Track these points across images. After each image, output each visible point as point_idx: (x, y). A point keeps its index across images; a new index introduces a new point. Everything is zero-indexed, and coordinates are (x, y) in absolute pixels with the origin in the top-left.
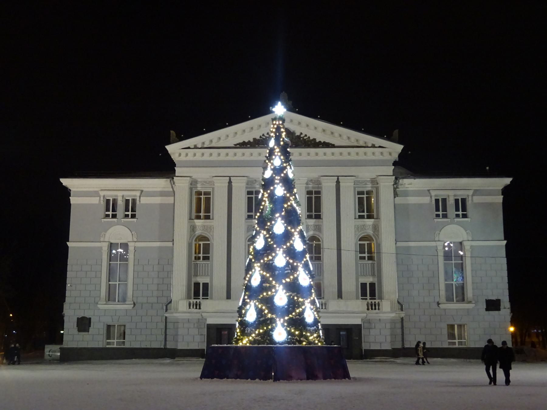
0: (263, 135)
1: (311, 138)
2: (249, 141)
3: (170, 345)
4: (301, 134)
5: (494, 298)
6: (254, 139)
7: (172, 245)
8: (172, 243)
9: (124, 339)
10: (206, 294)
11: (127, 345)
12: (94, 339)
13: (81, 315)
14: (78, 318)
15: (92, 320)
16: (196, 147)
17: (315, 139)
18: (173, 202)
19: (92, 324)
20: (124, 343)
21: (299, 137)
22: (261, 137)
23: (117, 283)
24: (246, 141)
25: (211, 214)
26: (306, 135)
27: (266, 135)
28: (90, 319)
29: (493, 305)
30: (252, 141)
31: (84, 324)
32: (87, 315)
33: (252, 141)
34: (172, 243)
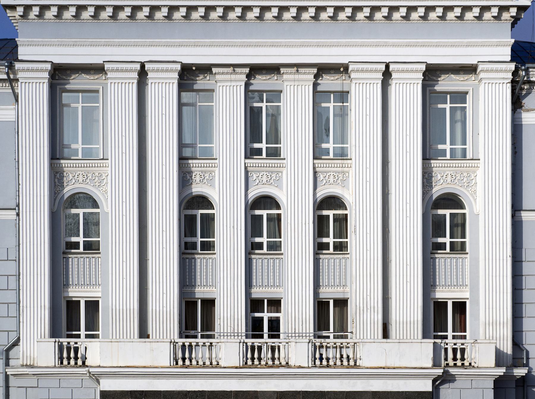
7: (15, 217)
8: (14, 213)
18: (13, 118)
34: (14, 213)
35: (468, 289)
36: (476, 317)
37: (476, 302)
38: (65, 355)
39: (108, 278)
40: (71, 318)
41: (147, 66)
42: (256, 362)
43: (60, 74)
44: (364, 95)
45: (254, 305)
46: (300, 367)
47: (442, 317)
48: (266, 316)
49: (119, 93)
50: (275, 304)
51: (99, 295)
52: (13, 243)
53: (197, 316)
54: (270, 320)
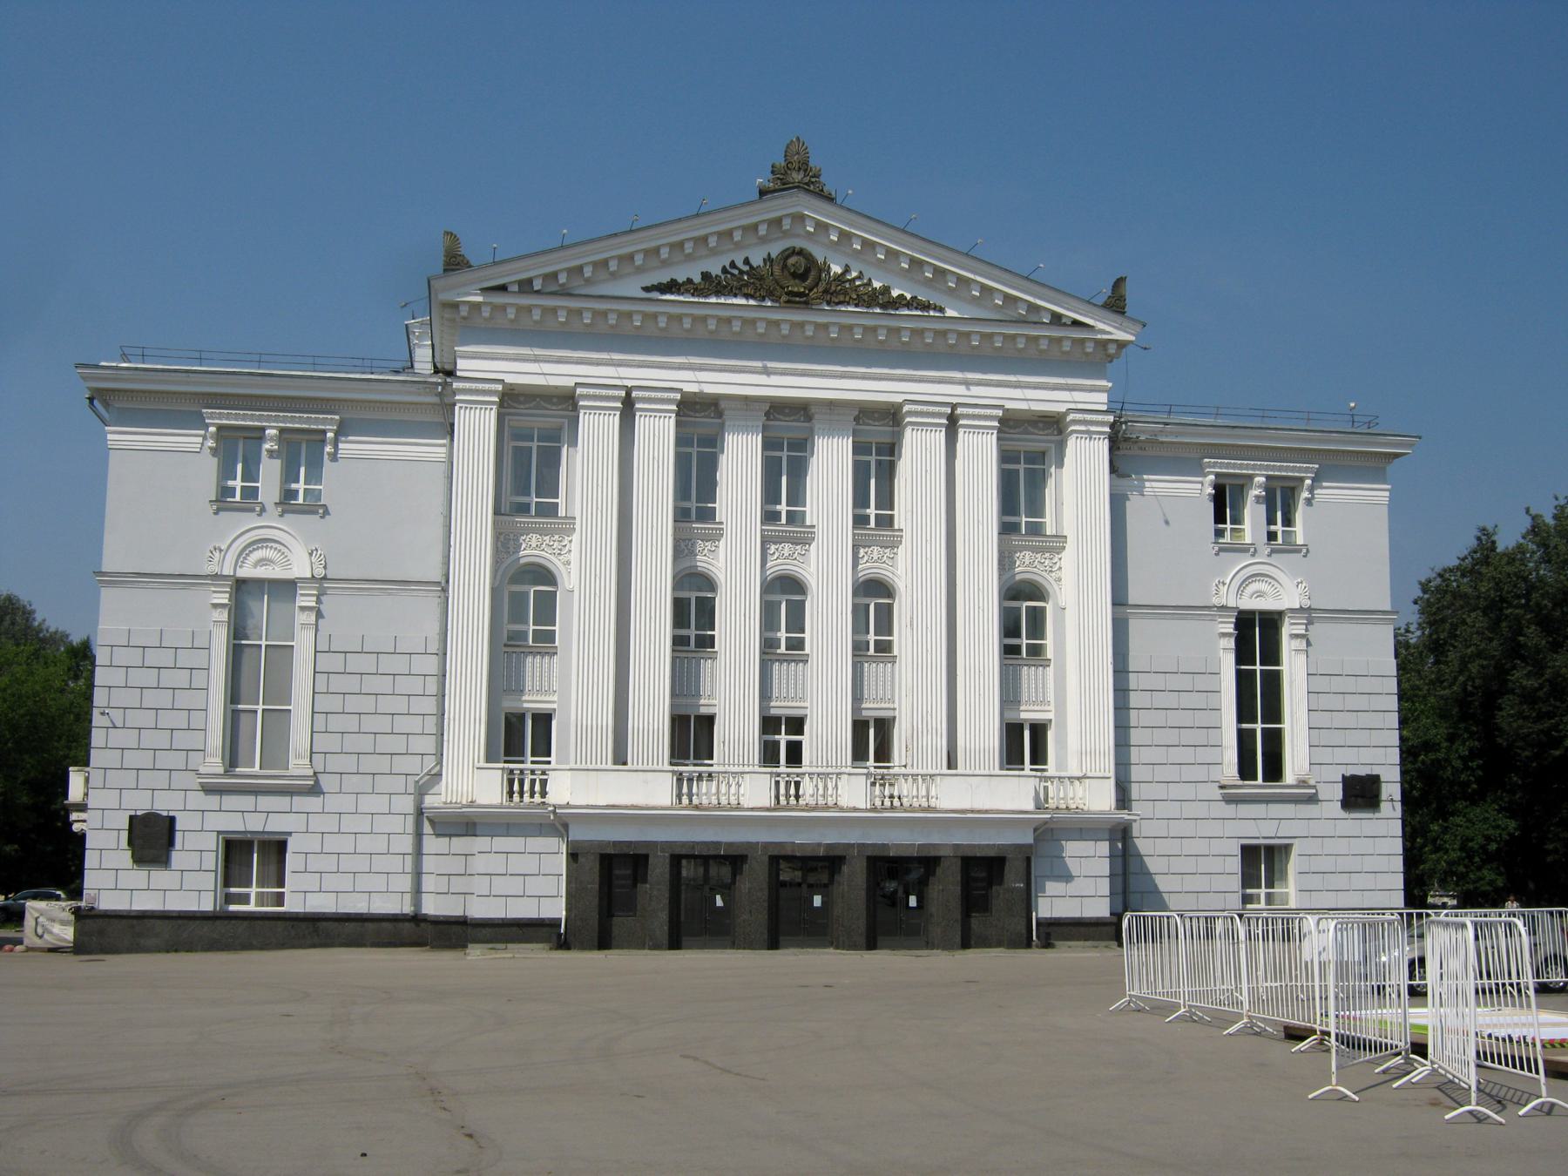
0: (733, 265)
1: (877, 284)
2: (690, 281)
3: (432, 907)
4: (847, 270)
5: (1362, 771)
6: (706, 276)
9: (281, 883)
10: (543, 747)
11: (292, 905)
12: (188, 884)
13: (141, 803)
14: (131, 818)
15: (178, 826)
16: (526, 286)
17: (886, 290)
19: (178, 836)
20: (279, 899)
21: (839, 279)
22: (724, 270)
23: (260, 707)
24: (681, 279)
25: (561, 501)
26: (860, 277)
27: (740, 264)
28: (172, 820)
29: (1360, 793)
30: (697, 279)
31: (152, 839)
32: (164, 804)
33: (697, 279)
35: (1052, 707)
36: (1063, 744)
37: (1063, 726)
38: (516, 787)
39: (572, 685)
40: (520, 735)
41: (634, 394)
42: (793, 801)
43: (512, 399)
44: (920, 450)
45: (769, 724)
46: (855, 809)
47: (1024, 743)
48: (783, 739)
49: (597, 430)
50: (796, 725)
51: (1050, 716)
52: (433, 630)
53: (692, 736)
54: (790, 744)
